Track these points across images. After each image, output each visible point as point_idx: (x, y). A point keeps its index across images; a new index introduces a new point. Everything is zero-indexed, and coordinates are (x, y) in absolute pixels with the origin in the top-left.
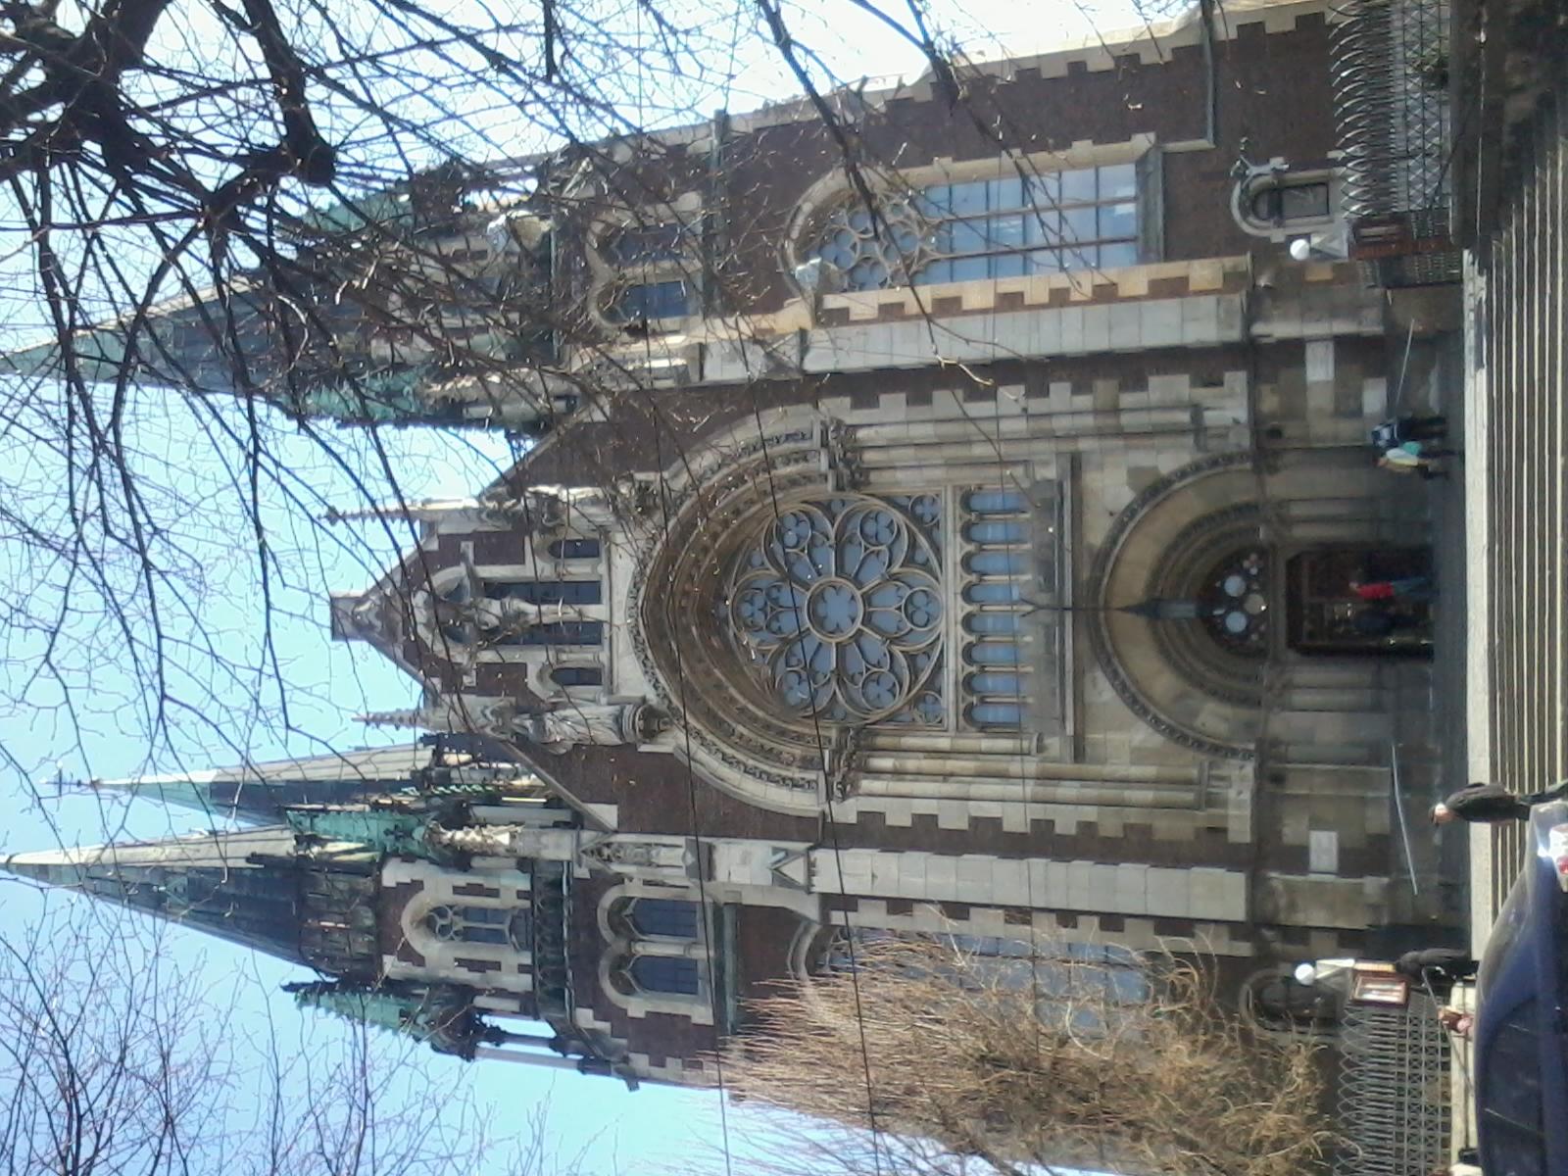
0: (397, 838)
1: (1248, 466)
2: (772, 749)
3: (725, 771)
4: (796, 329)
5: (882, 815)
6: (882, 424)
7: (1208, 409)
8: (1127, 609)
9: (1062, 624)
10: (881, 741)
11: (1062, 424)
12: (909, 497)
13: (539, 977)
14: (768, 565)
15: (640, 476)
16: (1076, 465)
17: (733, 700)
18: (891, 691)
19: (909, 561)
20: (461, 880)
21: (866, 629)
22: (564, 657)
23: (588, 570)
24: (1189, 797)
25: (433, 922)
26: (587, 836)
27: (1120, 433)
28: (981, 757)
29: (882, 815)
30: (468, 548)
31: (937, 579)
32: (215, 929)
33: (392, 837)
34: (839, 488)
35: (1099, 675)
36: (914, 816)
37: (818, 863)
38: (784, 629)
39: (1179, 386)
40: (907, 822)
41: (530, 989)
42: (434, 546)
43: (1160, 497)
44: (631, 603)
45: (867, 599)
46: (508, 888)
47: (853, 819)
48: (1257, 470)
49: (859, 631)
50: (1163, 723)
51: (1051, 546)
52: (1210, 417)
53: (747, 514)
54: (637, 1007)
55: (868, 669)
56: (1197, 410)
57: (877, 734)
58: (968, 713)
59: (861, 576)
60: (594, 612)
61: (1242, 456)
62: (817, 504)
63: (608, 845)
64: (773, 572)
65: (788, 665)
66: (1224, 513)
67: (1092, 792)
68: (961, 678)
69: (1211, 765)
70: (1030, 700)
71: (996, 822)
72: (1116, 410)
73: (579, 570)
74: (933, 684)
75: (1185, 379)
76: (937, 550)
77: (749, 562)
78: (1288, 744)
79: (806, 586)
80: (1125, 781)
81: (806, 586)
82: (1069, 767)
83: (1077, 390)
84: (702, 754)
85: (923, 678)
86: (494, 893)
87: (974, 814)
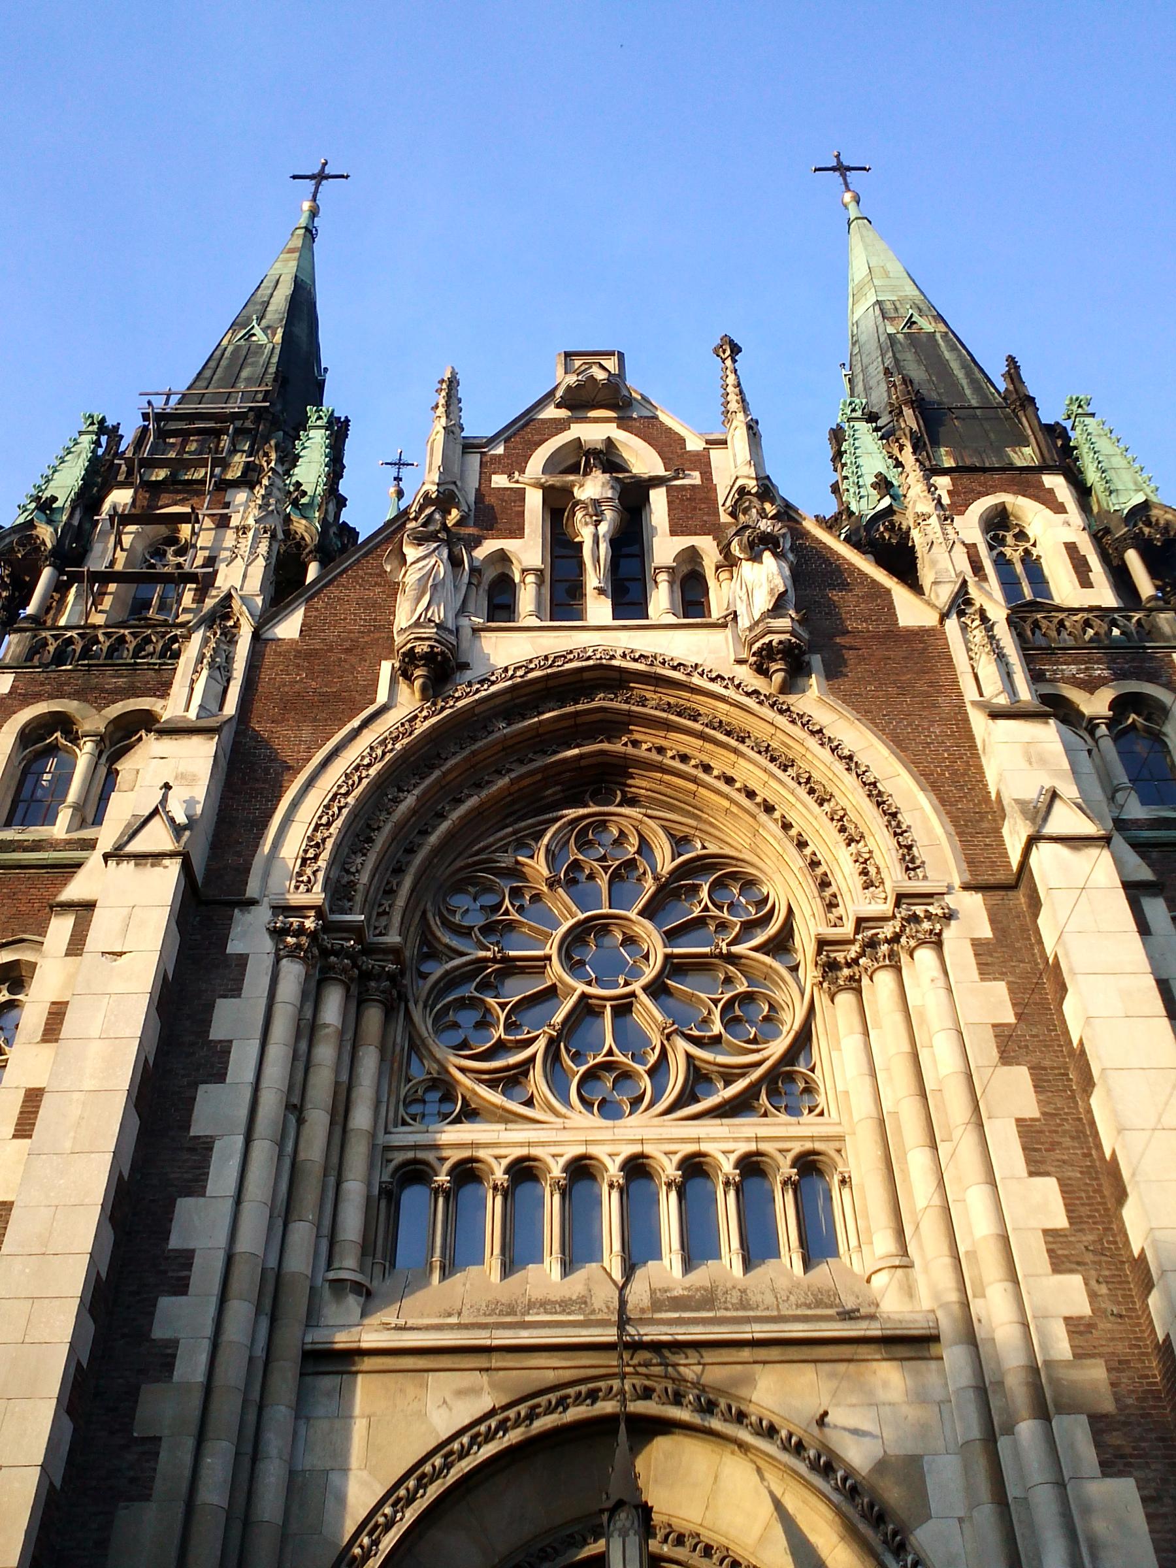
10: (374, 1016)
12: (812, 1070)
13: (69, 634)
28: (332, 1180)
29: (235, 990)
34: (822, 944)
35: (486, 1403)
40: (217, 1032)
47: (234, 947)
51: (743, 1305)
57: (389, 1013)
62: (787, 930)
63: (237, 625)
68: (481, 1154)
71: (196, 1185)
82: (292, 1338)
83: (1074, 1326)
84: (368, 737)
87: (217, 1145)
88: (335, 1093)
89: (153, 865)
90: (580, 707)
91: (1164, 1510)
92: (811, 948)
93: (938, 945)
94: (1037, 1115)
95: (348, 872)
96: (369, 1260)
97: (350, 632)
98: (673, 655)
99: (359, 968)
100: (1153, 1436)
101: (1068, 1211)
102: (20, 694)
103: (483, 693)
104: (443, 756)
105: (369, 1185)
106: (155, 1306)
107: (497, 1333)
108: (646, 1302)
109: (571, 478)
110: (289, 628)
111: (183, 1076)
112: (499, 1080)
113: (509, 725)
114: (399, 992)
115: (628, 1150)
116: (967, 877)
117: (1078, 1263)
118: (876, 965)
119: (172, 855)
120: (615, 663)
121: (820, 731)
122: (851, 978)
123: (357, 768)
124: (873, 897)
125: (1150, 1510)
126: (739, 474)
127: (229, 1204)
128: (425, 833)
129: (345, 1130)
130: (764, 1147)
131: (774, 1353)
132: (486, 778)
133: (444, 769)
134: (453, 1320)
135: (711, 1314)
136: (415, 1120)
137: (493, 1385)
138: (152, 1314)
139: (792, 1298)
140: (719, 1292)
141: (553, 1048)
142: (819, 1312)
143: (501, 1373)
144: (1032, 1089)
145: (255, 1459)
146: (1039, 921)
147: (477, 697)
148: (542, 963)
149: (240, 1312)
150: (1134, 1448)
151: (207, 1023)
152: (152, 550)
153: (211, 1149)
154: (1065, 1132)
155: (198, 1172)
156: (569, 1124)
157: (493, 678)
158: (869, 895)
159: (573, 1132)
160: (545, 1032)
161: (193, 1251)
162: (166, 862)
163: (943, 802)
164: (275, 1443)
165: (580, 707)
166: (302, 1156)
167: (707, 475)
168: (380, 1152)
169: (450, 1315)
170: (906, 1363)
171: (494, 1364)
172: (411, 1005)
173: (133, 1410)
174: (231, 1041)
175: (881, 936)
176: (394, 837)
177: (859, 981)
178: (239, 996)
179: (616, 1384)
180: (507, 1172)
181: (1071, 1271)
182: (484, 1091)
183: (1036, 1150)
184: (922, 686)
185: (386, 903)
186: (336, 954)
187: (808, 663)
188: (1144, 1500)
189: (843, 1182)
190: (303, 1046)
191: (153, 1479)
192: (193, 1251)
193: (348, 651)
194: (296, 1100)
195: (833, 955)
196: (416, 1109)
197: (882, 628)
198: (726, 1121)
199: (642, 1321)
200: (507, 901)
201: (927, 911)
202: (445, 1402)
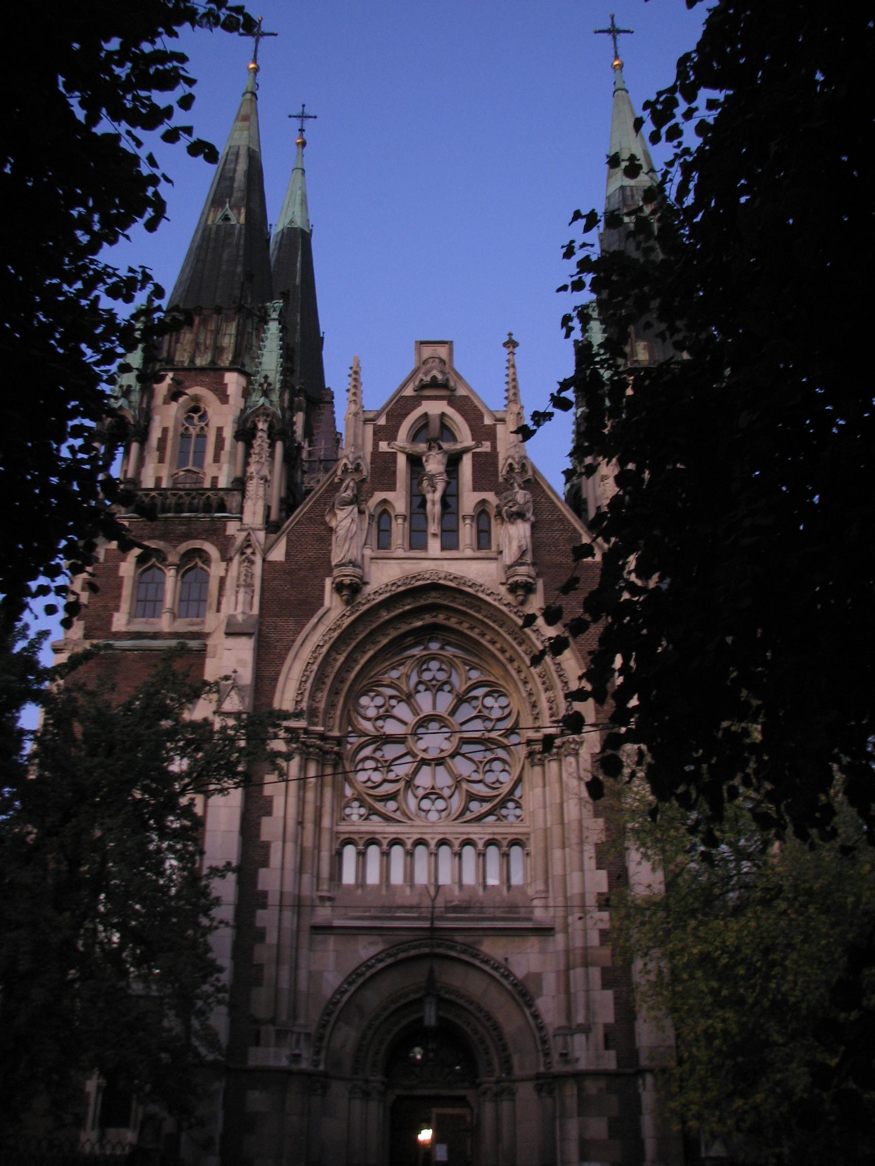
0: (261, 385)
1: (542, 1069)
2: (324, 683)
3: (310, 646)
7: (587, 1038)
8: (431, 971)
10: (329, 770)
14: (470, 683)
15: (540, 584)
19: (471, 797)
20: (228, 434)
23: (468, 541)
24: (284, 1017)
25: (196, 409)
26: (261, 535)
27: (568, 968)
30: (486, 447)
31: (455, 819)
32: (196, 244)
33: (262, 380)
35: (380, 947)
36: (271, 797)
39: (606, 1014)
41: (144, 486)
42: (488, 421)
43: (518, 998)
45: (439, 762)
46: (220, 469)
48: (538, 1076)
50: (341, 997)
52: (579, 1040)
53: (509, 667)
56: (586, 1029)
57: (335, 766)
60: (434, 546)
61: (548, 1065)
62: (517, 723)
63: (253, 553)
64: (464, 688)
65: (391, 697)
66: (505, 1048)
67: (287, 939)
68: (378, 836)
69: (308, 1035)
71: (265, 863)
72: (586, 964)
73: (467, 532)
75: (610, 1019)
76: (479, 819)
79: (453, 713)
80: (295, 968)
81: (453, 713)
82: (306, 923)
83: (603, 934)
84: (322, 629)
85: (379, 806)
86: (217, 459)
93: (576, 754)
103: (376, 601)
113: (389, 613)
120: (441, 582)
121: (537, 630)
122: (540, 759)
127: (279, 872)
131: (491, 933)
133: (357, 640)
134: (367, 914)
142: (511, 915)
147: (373, 603)
149: (288, 915)
156: (414, 823)
157: (380, 591)
164: (303, 963)
167: (494, 447)
168: (335, 834)
185: (332, 712)
188: (616, 998)
190: (301, 793)
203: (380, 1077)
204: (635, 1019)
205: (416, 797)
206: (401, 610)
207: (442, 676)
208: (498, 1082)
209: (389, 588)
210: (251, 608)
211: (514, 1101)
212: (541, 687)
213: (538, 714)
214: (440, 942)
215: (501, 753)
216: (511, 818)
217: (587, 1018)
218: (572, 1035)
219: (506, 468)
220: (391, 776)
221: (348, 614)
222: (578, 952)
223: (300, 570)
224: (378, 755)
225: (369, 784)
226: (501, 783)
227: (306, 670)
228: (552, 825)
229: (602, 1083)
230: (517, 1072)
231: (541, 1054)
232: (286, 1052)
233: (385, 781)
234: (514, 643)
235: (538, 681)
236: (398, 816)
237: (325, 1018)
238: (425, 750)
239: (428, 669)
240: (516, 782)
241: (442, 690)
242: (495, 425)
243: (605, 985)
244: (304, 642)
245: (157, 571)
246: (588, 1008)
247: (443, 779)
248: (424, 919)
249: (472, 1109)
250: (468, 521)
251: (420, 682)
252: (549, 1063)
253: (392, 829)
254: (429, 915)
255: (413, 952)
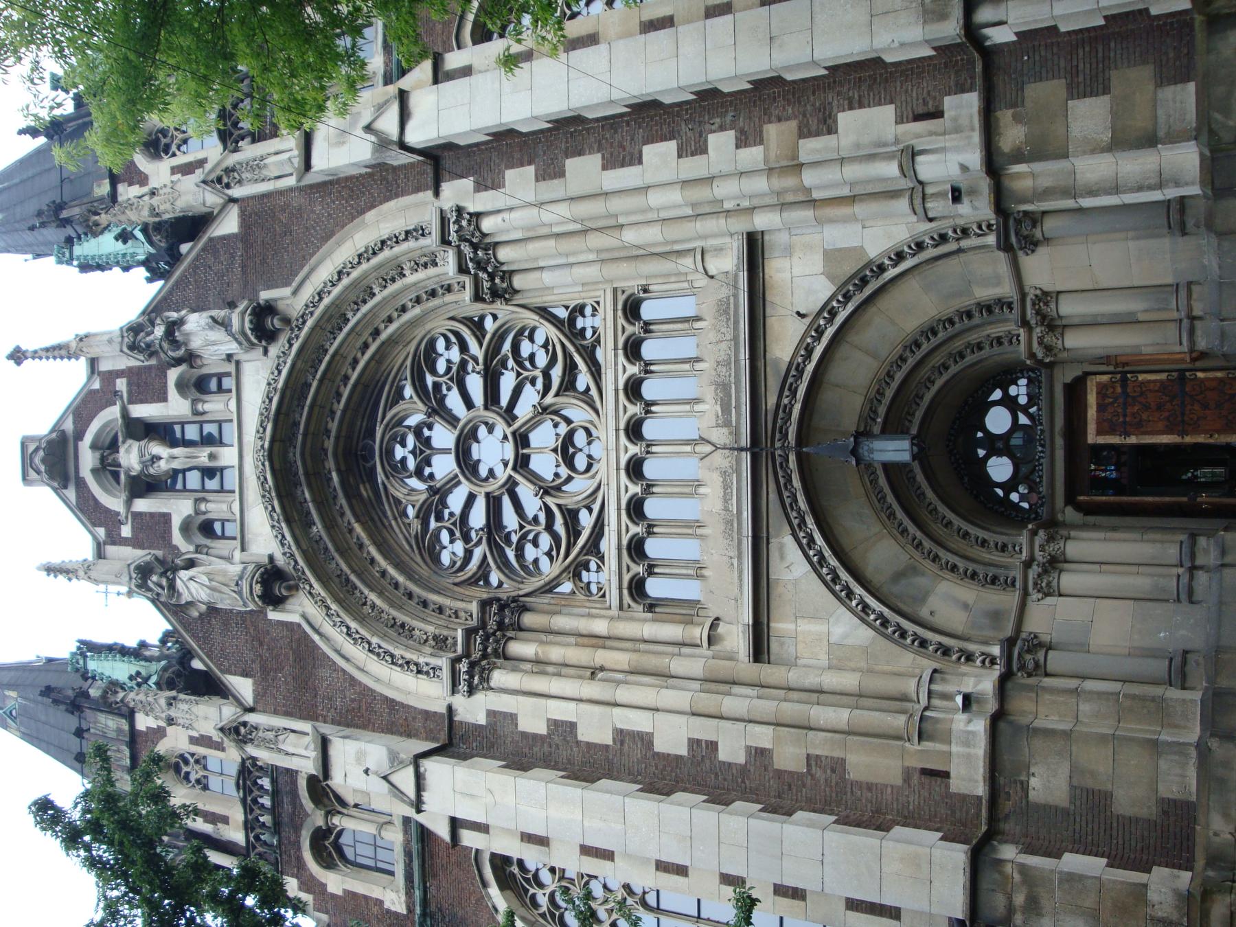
1: (991, 239)
4: (397, 92)
5: (513, 717)
6: (511, 209)
9: (738, 472)
10: (528, 619)
11: (726, 190)
14: (415, 398)
16: (755, 248)
17: (373, 561)
18: (549, 554)
21: (518, 477)
22: (203, 507)
28: (643, 646)
29: (513, 717)
30: (121, 384)
34: (478, 298)
35: (789, 540)
37: (428, 775)
38: (438, 476)
40: (542, 729)
42: (96, 385)
43: (868, 291)
44: (261, 443)
47: (482, 720)
48: (1005, 246)
49: (510, 477)
52: (927, 168)
53: (384, 336)
54: (336, 882)
55: (522, 527)
56: (909, 155)
57: (525, 609)
58: (637, 588)
59: (517, 411)
61: (983, 228)
63: (245, 724)
64: (420, 405)
65: (439, 518)
67: (767, 707)
68: (625, 542)
70: (705, 572)
71: (645, 740)
72: (798, 167)
74: (593, 546)
75: (888, 111)
77: (399, 396)
78: (1049, 647)
79: (452, 420)
80: (818, 693)
84: (327, 628)
87: (619, 726)
88: (583, 646)
89: (424, 779)
90: (301, 471)
91: (856, 96)
92: (479, 306)
93: (478, 216)
94: (599, 156)
95: (426, 641)
96: (695, 619)
97: (247, 642)
98: (260, 401)
99: (495, 631)
100: (812, 98)
101: (666, 140)
102: (298, 871)
103: (292, 544)
104: (339, 572)
105: (645, 620)
106: (724, 763)
107: (745, 533)
108: (725, 431)
109: (123, 477)
110: (244, 687)
111: (572, 750)
112: (574, 529)
113: (314, 524)
114: (513, 602)
115: (623, 439)
116: (429, 194)
117: (701, 136)
118: (493, 260)
119: (417, 768)
120: (267, 445)
121: (319, 294)
122: (502, 279)
123: (349, 635)
124: (444, 259)
125: (857, 105)
126: (118, 349)
127: (658, 715)
128: (397, 585)
129: (609, 638)
130: (620, 345)
132: (355, 540)
133: (348, 572)
134: (735, 562)
135: (733, 386)
136: (601, 589)
137: (777, 536)
138: (730, 764)
139: (723, 330)
140: (719, 380)
141: (552, 492)
142: (732, 313)
143: (770, 530)
144: (582, 157)
145: (822, 692)
146: (462, 144)
147: (294, 548)
148: (491, 500)
150: (820, 111)
151: (535, 737)
152: (185, 782)
153: (622, 731)
154: (612, 137)
155: (637, 738)
158: (442, 263)
159: (610, 478)
160: (541, 498)
161: (689, 739)
162: (422, 769)
163: (373, 207)
164: (811, 680)
165: (301, 471)
166: (626, 667)
167: (119, 374)
169: (732, 564)
170: (766, 256)
171: (765, 535)
172: (521, 593)
173: (790, 772)
174: (548, 720)
175: (472, 255)
176: (400, 608)
177: (504, 272)
178: (516, 715)
179: (779, 452)
180: (637, 524)
181: (706, 141)
182: (581, 541)
183: (624, 158)
184: (284, 218)
185: (448, 612)
186: (485, 648)
187: (267, 301)
188: (851, 108)
189: (645, 291)
190: (550, 669)
191: (832, 758)
192: (689, 739)
193: (261, 644)
194: (588, 673)
195: (486, 290)
196: (594, 588)
197: (240, 245)
198: (603, 371)
199: (737, 434)
200: (447, 524)
201: (454, 223)
202: (788, 567)
203: (1023, 539)
204: (877, 62)
205: (569, 479)
206: (310, 504)
207: (411, 440)
208: (1025, 323)
209: (275, 524)
210: (308, 734)
211: (1059, 293)
212: (399, 284)
213: (442, 287)
214: (778, 436)
215: (507, 346)
216: (597, 322)
217: (889, 157)
218: (920, 183)
219: (135, 354)
220: (542, 517)
221: (307, 587)
222: (779, 183)
223: (261, 656)
224: (514, 538)
225: (554, 553)
226: (547, 339)
227: (378, 655)
228: (590, 250)
229: (1005, 116)
230: (1006, 289)
231: (965, 243)
232: (960, 721)
233: (549, 527)
234: (346, 330)
235: (392, 288)
236: (596, 508)
237: (909, 641)
238: (506, 465)
239: (404, 459)
240: (542, 317)
241: (429, 438)
242: (99, 375)
243: (831, 130)
244: (343, 657)
245: (342, 840)
246: (872, 157)
247: (544, 437)
248: (738, 461)
249: (1087, 374)
250: (200, 407)
251: (419, 473)
252: (980, 227)
253: (614, 519)
254: (736, 453)
255: (796, 483)
